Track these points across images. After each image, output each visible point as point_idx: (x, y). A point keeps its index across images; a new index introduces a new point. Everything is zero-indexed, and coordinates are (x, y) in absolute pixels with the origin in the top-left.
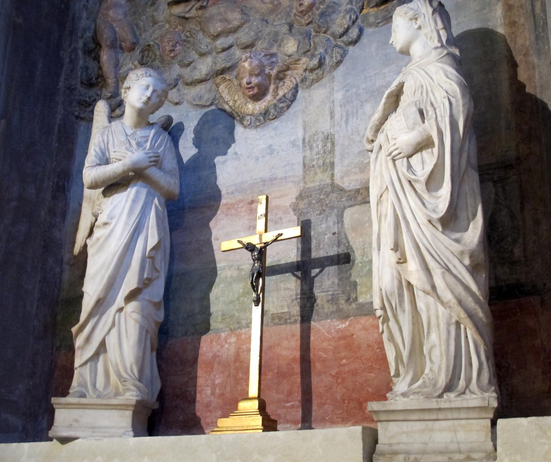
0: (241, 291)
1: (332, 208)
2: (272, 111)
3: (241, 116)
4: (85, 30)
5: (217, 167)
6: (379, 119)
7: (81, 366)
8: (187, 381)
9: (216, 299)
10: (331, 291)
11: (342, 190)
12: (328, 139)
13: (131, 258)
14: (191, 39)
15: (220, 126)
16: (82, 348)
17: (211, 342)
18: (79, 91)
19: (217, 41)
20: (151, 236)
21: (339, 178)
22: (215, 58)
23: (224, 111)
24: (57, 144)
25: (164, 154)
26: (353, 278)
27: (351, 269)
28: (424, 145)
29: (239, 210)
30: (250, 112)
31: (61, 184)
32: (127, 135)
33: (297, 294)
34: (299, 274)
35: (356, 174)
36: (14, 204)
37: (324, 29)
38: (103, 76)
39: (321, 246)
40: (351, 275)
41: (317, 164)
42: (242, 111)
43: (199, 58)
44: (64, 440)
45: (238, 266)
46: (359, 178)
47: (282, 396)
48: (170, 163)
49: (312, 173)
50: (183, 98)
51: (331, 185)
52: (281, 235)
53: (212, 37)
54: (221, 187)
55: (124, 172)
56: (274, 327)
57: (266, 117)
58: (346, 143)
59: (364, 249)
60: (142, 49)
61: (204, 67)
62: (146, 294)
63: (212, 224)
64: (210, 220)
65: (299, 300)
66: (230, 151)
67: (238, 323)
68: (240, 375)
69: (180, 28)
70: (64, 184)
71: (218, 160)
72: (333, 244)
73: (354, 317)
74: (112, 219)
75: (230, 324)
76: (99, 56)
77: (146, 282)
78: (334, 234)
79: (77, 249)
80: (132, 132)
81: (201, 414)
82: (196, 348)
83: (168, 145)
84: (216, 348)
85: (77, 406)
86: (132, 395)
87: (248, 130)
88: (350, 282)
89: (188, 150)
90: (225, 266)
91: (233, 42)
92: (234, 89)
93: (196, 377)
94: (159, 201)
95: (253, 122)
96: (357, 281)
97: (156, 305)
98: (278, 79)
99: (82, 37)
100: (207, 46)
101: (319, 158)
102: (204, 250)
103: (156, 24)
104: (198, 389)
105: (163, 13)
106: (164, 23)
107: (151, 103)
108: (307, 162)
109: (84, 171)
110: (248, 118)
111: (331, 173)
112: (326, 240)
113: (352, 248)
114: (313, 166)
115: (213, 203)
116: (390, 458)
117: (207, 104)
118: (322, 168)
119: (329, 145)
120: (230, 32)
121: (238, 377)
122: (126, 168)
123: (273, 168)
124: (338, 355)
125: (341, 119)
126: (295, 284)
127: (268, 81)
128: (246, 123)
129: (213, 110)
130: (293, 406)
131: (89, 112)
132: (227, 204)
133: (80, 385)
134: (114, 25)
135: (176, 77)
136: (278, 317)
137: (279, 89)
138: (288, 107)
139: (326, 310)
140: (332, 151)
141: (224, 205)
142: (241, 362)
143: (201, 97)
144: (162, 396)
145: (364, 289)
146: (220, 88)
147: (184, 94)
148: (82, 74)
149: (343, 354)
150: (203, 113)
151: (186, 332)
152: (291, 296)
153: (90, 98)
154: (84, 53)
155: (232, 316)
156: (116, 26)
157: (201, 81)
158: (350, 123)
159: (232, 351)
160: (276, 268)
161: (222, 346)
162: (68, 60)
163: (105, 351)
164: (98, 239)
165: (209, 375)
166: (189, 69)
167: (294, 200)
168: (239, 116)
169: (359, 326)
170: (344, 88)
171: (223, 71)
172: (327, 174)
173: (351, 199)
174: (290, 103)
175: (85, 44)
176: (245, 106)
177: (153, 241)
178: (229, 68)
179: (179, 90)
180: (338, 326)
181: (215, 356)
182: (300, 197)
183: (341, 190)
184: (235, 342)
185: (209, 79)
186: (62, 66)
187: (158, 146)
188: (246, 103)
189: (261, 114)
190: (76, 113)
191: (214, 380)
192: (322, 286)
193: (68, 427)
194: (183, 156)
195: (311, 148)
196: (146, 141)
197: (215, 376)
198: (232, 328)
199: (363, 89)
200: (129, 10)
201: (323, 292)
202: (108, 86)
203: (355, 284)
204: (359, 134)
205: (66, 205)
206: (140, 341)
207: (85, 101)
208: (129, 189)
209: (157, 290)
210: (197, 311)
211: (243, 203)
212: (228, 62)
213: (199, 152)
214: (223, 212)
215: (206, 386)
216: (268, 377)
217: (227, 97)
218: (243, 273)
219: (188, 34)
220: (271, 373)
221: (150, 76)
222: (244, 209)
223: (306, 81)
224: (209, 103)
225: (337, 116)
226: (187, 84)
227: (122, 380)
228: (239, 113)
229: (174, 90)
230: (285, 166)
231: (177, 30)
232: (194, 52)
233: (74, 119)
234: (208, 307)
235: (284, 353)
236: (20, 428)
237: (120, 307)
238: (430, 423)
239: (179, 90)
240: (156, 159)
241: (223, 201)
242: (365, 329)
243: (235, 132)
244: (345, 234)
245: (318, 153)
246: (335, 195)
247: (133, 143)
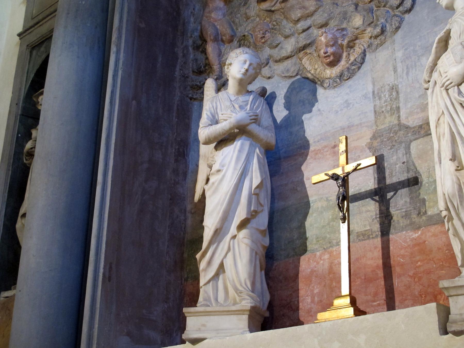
0: (331, 217)
1: (401, 143)
2: (346, 73)
3: (321, 81)
4: (193, 31)
5: (305, 122)
7: (205, 284)
8: (291, 294)
9: (311, 226)
10: (404, 209)
11: (407, 127)
13: (240, 196)
14: (277, 27)
15: (305, 91)
16: (205, 270)
17: (309, 259)
18: (192, 78)
19: (298, 24)
20: (255, 177)
21: (404, 119)
22: (298, 38)
23: (308, 78)
24: (176, 120)
25: (261, 115)
26: (421, 197)
27: (420, 189)
29: (325, 154)
30: (328, 76)
31: (181, 150)
32: (231, 101)
33: (376, 215)
34: (377, 198)
36: (146, 166)
37: (383, 4)
38: (209, 65)
39: (394, 174)
40: (420, 194)
42: (322, 77)
43: (284, 40)
44: (195, 341)
45: (327, 198)
47: (369, 297)
48: (266, 120)
49: (382, 117)
50: (274, 73)
51: (399, 125)
52: (360, 165)
53: (294, 22)
54: (309, 138)
55: (231, 129)
56: (359, 243)
57: (342, 78)
58: (409, 90)
59: (429, 171)
60: (239, 39)
61: (289, 46)
62: (253, 223)
63: (303, 168)
64: (302, 165)
65: (378, 219)
66: (314, 109)
67: (330, 243)
68: (334, 284)
69: (268, 19)
70: (184, 152)
71: (305, 117)
73: (425, 227)
74: (223, 166)
75: (323, 245)
76: (205, 49)
77: (254, 214)
78: (404, 163)
79: (197, 197)
80: (235, 98)
81: (304, 319)
82: (297, 266)
83: (264, 107)
84: (313, 265)
85: (203, 314)
86: (247, 303)
87: (327, 91)
88: (420, 199)
89: (280, 112)
90: (316, 200)
91: (311, 24)
92: (314, 60)
93: (298, 290)
94: (260, 150)
95: (331, 84)
96: (426, 198)
97: (263, 232)
98: (349, 47)
99: (191, 37)
100: (290, 29)
101: (387, 105)
102: (299, 189)
103: (249, 19)
104: (301, 299)
105: (254, 10)
106: (255, 18)
107: (248, 74)
108: (377, 109)
109: (199, 131)
110: (327, 81)
111: (397, 115)
112: (397, 169)
113: (419, 173)
114: (383, 112)
115: (303, 151)
116: (461, 325)
117: (293, 75)
118: (390, 113)
119: (394, 94)
120: (308, 16)
121: (332, 286)
122: (232, 126)
123: (350, 118)
124: (414, 259)
126: (374, 207)
127: (341, 50)
128: (325, 85)
129: (299, 79)
130: (379, 305)
131: (200, 93)
132: (314, 150)
133: (205, 300)
134: (216, 24)
135: (267, 57)
136: (362, 234)
137: (351, 55)
138: (359, 68)
139: (402, 225)
140: (397, 98)
141: (312, 151)
142: (334, 273)
143: (288, 70)
144: (271, 306)
145: (431, 204)
146: (303, 61)
147: (274, 70)
148: (193, 64)
149: (418, 258)
150: (290, 83)
151: (288, 255)
152: (372, 216)
153: (200, 82)
154: (194, 49)
155: (324, 238)
156: (218, 25)
157: (288, 58)
158: (410, 74)
159: (327, 265)
160: (358, 196)
161: (318, 263)
162: (181, 54)
163: (224, 272)
164: (213, 183)
165: (309, 287)
166: (277, 49)
167: (369, 141)
168: (320, 81)
169: (429, 234)
170: (403, 47)
171: (304, 47)
172: (394, 116)
174: (360, 65)
175: (194, 42)
176: (324, 72)
177: (257, 181)
178: (309, 44)
179: (270, 67)
180: (412, 235)
181: (312, 272)
182: (374, 137)
183: (407, 128)
184: (328, 258)
185: (294, 56)
186: (177, 59)
187: (256, 108)
188: (325, 69)
189: (337, 76)
190: (190, 95)
191: (312, 291)
192: (397, 205)
193: (197, 331)
194: (276, 118)
195: (380, 98)
196: (247, 104)
197: (313, 287)
198: (325, 248)
199: (419, 46)
200: (227, 11)
201: (397, 210)
202: (214, 71)
203: (424, 201)
205: (187, 166)
206: (251, 261)
207: (196, 85)
208: (235, 143)
209: (263, 220)
210: (295, 238)
211: (327, 148)
212: (308, 39)
213: (289, 113)
214: (312, 157)
215: (307, 296)
216: (357, 283)
217: (309, 67)
218: (331, 203)
219: (274, 23)
220: (359, 280)
221: (247, 53)
222: (328, 153)
223: (372, 46)
224: (295, 74)
225: (399, 70)
226: (276, 61)
227: (238, 292)
228: (320, 79)
229: (266, 68)
230: (360, 114)
231: (265, 21)
232: (280, 36)
233: (189, 100)
234: (305, 233)
235: (369, 262)
236: (160, 342)
237: (234, 235)
239: (270, 67)
240: (256, 117)
241: (312, 148)
242: (435, 235)
243: (318, 94)
244: (413, 162)
245: (386, 101)
246: (402, 132)
247: (237, 106)
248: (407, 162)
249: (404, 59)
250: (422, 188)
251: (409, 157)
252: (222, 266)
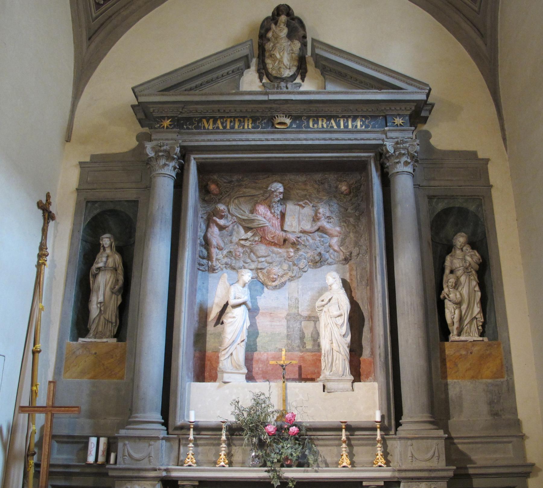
28: (340, 315)
140: (298, 303)
159: (265, 358)
171: (261, 269)
175: (201, 242)
181: (259, 359)
182: (288, 315)
203: (305, 343)
225: (300, 293)
241: (260, 311)
242: (308, 356)
246: (298, 317)
252: (232, 354)
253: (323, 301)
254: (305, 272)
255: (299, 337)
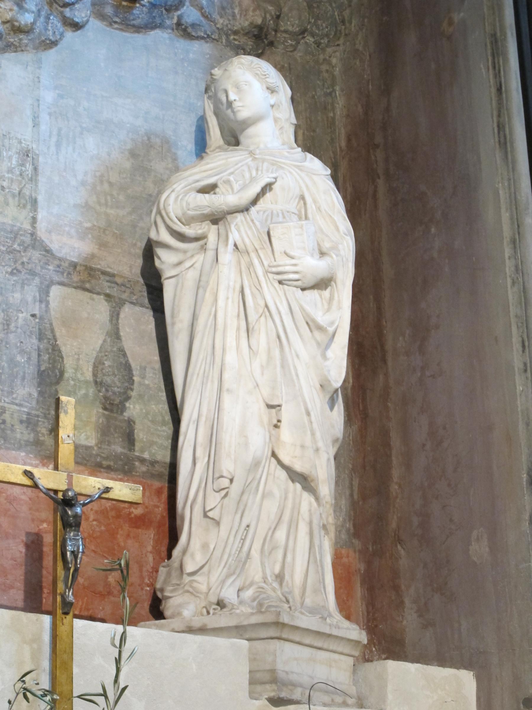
1: (33, 273)
6: (234, 206)
10: (26, 407)
11: (48, 251)
12: (28, 155)
28: (323, 284)
35: (72, 237)
41: (9, 188)
46: (76, 245)
51: (32, 235)
59: (78, 359)
72: (31, 332)
78: (33, 316)
101: (12, 180)
111: (31, 215)
112: (20, 321)
113: (60, 352)
118: (17, 199)
119: (29, 167)
125: (50, 137)
140: (34, 179)
172: (25, 213)
173: (62, 273)
192: (12, 393)
201: (13, 403)
204: (75, 176)
225: (43, 127)
238: (314, 651)
244: (51, 324)
245: (10, 170)
246: (36, 255)
248: (41, 318)
249: (55, 112)
250: (63, 384)
251: (46, 311)
253: (209, 189)
254: (76, 26)
255: (31, 370)
